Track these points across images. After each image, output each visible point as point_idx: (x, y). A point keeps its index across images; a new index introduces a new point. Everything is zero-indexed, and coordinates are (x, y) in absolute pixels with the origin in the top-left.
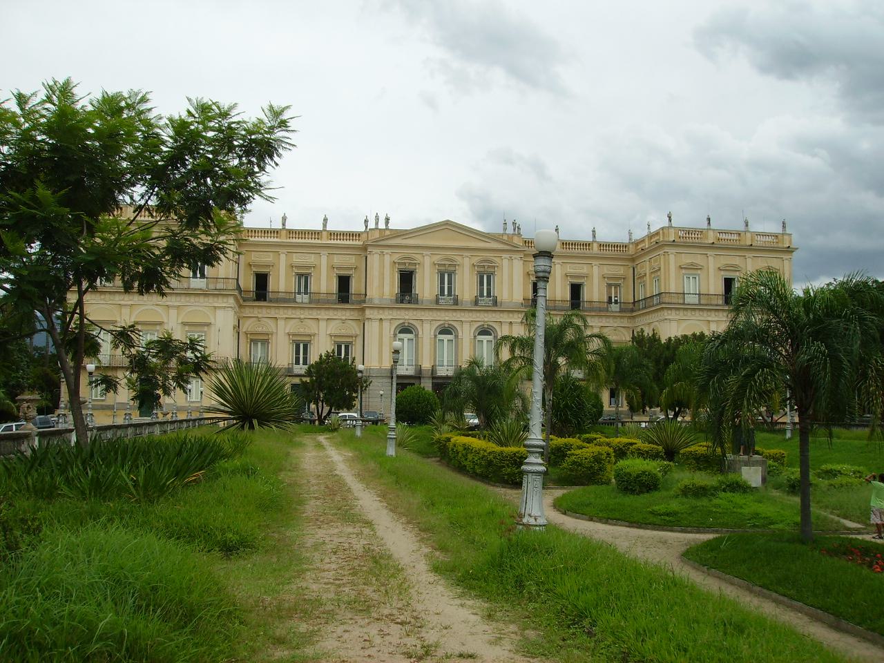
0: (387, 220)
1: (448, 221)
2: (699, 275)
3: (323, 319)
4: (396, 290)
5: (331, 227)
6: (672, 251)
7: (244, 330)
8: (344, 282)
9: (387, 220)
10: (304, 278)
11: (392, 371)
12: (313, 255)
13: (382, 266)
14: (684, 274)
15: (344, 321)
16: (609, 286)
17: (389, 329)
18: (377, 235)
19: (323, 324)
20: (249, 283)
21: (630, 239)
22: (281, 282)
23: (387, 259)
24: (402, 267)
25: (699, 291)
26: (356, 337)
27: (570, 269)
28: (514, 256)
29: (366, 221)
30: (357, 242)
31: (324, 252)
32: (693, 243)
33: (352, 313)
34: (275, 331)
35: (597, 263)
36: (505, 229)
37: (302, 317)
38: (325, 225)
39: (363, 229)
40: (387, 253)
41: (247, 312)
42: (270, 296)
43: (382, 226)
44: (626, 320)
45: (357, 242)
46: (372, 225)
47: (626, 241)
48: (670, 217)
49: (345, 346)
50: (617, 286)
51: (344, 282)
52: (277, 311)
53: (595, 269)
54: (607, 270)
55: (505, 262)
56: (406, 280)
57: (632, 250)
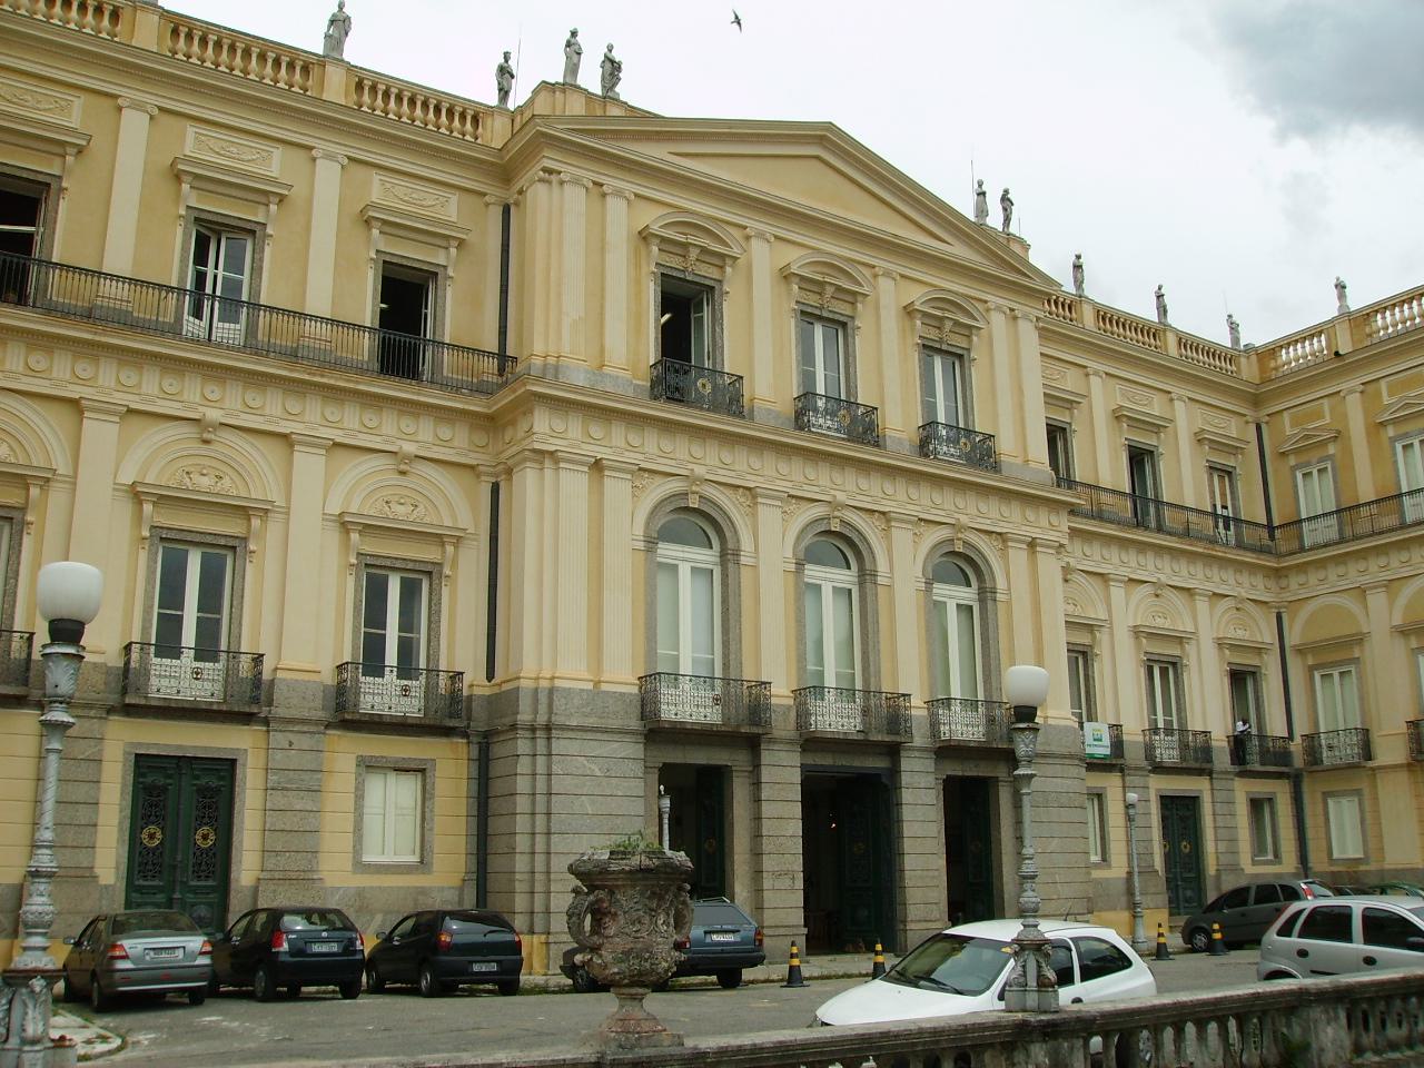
1: (830, 126)
3: (313, 442)
4: (651, 351)
8: (405, 297)
11: (647, 703)
15: (403, 464)
17: (628, 511)
19: (309, 465)
24: (675, 262)
26: (458, 541)
28: (1020, 309)
33: (445, 432)
34: (63, 468)
37: (213, 415)
42: (58, 287)
44: (1259, 581)
49: (404, 582)
51: (405, 297)
56: (683, 310)
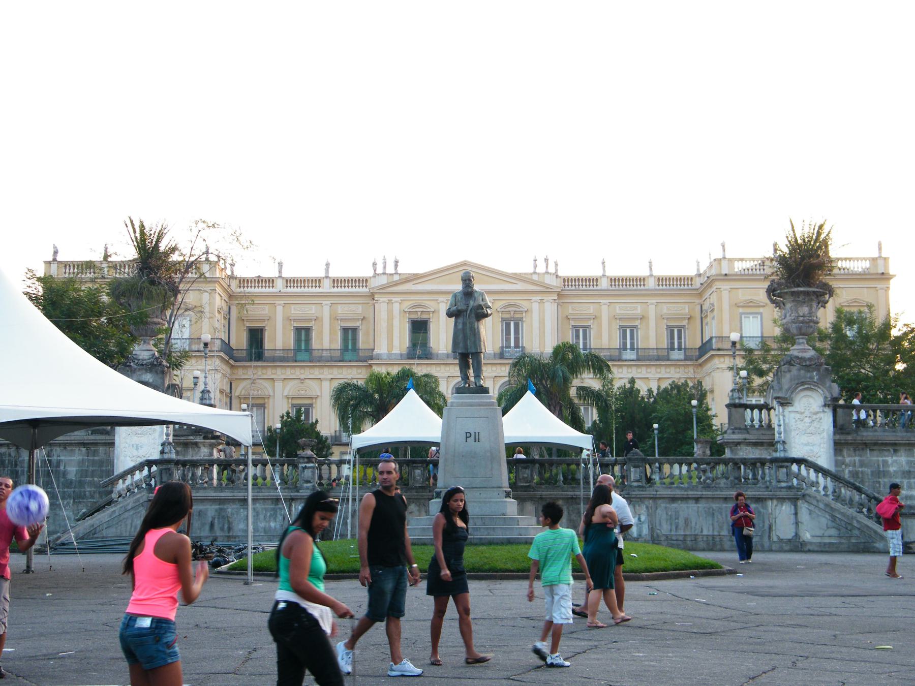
0: (396, 262)
2: (761, 314)
3: (326, 379)
4: (407, 343)
5: (333, 274)
6: (725, 286)
7: (237, 394)
9: (396, 262)
10: (303, 334)
12: (313, 306)
13: (390, 318)
14: (741, 314)
16: (671, 330)
18: (383, 280)
20: (240, 341)
21: (698, 270)
22: (279, 339)
23: (396, 307)
24: (414, 316)
25: (762, 333)
27: (619, 310)
29: (374, 264)
30: (361, 290)
31: (327, 302)
32: (753, 275)
33: (359, 371)
34: (271, 394)
35: (654, 301)
36: (535, 267)
37: (302, 377)
38: (327, 271)
39: (370, 273)
40: (396, 302)
41: (240, 373)
42: (267, 354)
43: (390, 269)
45: (361, 290)
46: (380, 270)
47: (692, 272)
48: (723, 246)
50: (680, 329)
52: (274, 371)
53: (652, 309)
54: (665, 310)
55: (535, 306)
57: (697, 283)
